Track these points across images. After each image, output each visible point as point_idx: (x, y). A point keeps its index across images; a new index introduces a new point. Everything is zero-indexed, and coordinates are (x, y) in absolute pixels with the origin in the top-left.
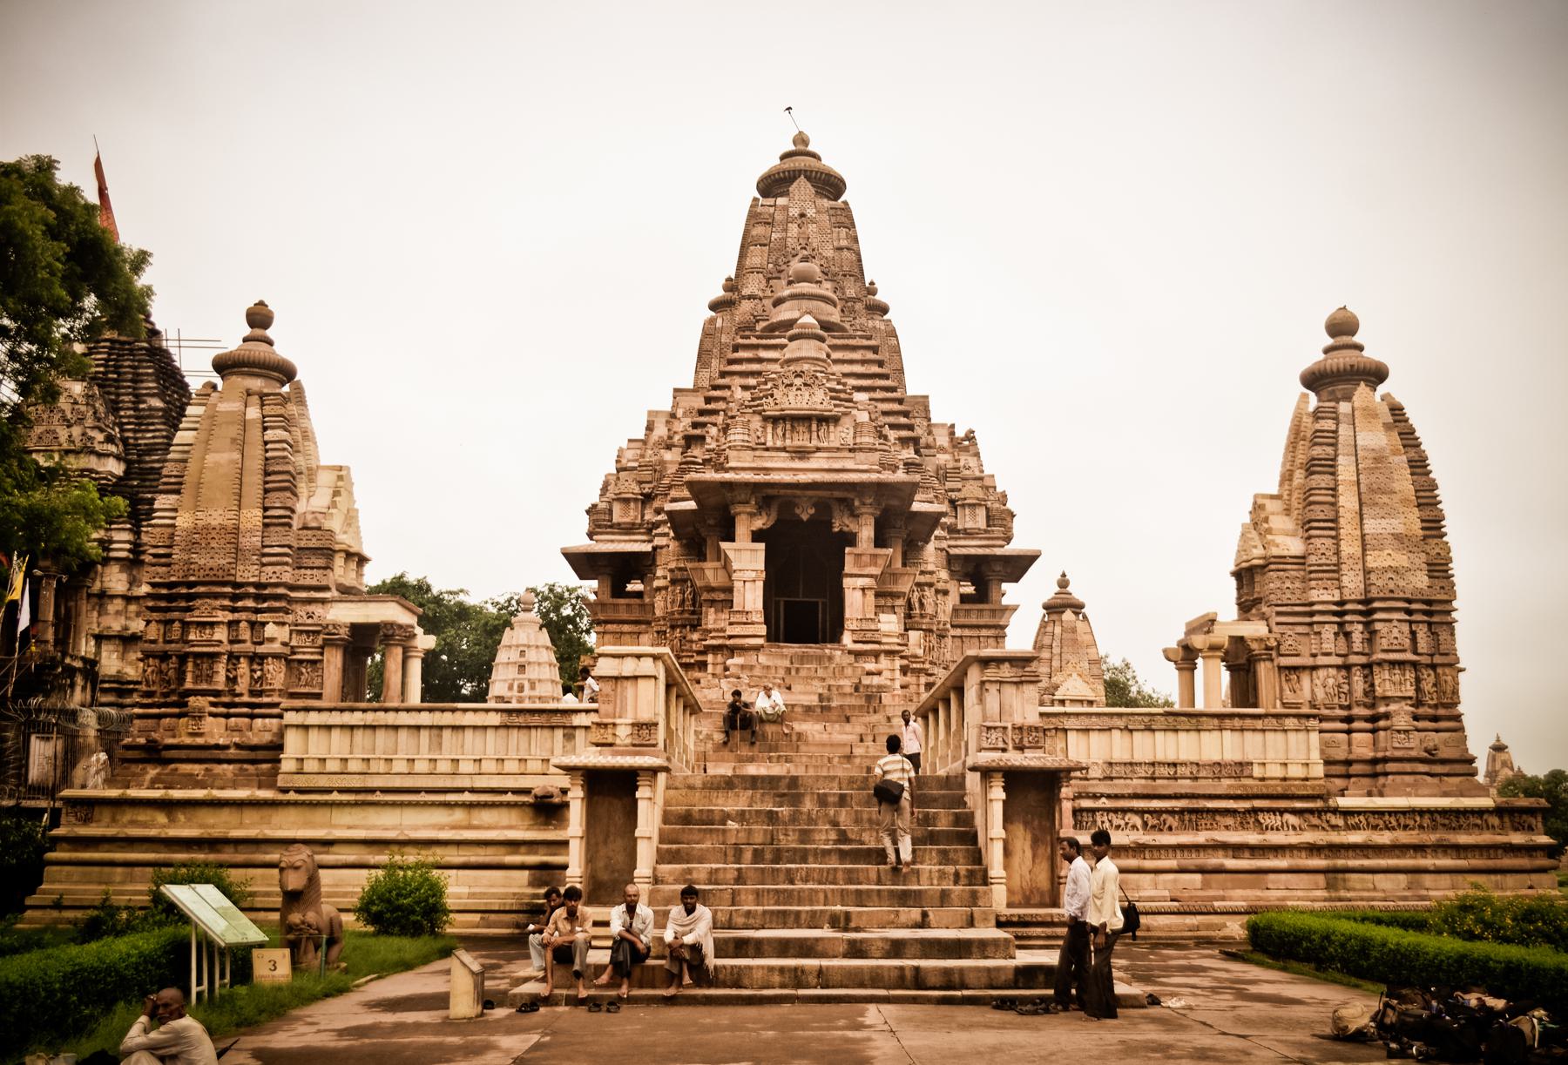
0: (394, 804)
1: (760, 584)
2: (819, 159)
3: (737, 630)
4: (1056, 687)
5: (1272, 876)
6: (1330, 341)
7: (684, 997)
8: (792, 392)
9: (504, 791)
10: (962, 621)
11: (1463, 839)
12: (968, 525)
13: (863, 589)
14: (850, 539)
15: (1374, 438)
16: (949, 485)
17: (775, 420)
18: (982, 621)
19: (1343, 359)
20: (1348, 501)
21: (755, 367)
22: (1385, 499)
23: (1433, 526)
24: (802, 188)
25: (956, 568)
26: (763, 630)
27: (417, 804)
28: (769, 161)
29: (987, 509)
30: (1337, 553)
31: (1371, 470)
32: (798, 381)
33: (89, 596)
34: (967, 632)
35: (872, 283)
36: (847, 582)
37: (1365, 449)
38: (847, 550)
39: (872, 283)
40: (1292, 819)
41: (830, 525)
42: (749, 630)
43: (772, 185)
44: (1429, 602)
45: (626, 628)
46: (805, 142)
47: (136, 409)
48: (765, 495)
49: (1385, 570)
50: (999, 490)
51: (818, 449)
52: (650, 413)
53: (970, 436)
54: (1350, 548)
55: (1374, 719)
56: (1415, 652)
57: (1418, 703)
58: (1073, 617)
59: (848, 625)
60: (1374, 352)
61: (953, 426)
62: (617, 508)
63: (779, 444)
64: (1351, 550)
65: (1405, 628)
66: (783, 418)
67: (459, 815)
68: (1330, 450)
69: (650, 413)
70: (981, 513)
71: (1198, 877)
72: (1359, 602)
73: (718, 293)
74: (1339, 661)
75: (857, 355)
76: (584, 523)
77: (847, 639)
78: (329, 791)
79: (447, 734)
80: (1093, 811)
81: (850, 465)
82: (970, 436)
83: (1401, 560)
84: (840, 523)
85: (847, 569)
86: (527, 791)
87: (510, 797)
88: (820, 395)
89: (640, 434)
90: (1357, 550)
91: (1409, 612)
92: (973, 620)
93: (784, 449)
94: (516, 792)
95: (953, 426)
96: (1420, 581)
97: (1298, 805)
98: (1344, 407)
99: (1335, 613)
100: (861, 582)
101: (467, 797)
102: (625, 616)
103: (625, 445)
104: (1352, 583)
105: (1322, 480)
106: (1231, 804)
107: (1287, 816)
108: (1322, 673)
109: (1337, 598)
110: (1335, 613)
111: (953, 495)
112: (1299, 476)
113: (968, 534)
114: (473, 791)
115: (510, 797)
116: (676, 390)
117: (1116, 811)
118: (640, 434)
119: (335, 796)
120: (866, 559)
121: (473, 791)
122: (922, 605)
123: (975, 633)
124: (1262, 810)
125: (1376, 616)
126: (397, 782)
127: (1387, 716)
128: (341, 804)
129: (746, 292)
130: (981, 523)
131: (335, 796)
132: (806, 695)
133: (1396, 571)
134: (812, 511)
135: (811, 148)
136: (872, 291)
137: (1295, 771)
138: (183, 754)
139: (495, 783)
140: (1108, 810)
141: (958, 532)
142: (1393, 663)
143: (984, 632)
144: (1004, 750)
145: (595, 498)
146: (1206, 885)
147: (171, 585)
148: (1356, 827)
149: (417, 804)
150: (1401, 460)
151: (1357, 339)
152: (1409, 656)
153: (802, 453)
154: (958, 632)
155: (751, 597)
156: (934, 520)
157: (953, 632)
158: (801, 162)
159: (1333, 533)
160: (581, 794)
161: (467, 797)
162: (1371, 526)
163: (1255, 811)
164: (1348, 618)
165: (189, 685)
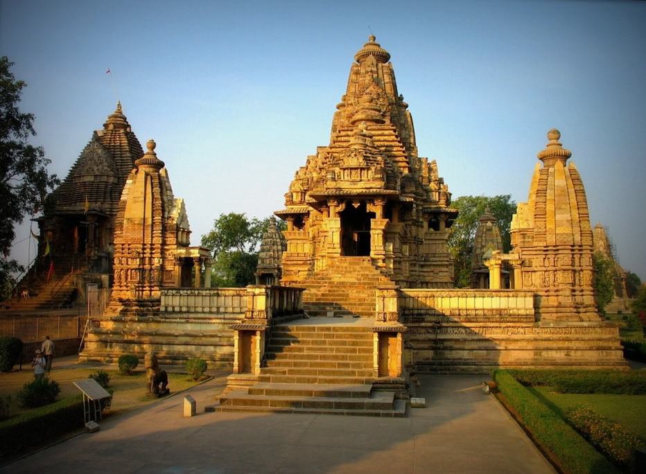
1: (339, 233)
2: (379, 46)
3: (330, 251)
4: (484, 253)
5: (512, 351)
6: (549, 142)
7: (340, 371)
8: (350, 158)
10: (428, 238)
11: (587, 337)
14: (373, 215)
15: (560, 182)
17: (344, 169)
18: (436, 238)
19: (554, 149)
20: (550, 207)
21: (346, 138)
22: (563, 206)
23: (584, 217)
24: (371, 59)
26: (339, 251)
28: (359, 48)
30: (545, 228)
31: (559, 195)
32: (353, 155)
33: (106, 229)
34: (431, 242)
35: (401, 95)
36: (372, 232)
37: (557, 186)
39: (401, 95)
40: (522, 330)
41: (366, 209)
42: (334, 251)
43: (361, 59)
44: (581, 246)
45: (299, 242)
46: (374, 39)
47: (121, 157)
48: (340, 198)
49: (563, 234)
51: (361, 181)
52: (308, 157)
53: (434, 162)
54: (550, 226)
55: (557, 291)
56: (573, 266)
57: (573, 285)
58: (491, 224)
59: (371, 248)
60: (567, 147)
61: (427, 158)
62: (294, 194)
63: (346, 178)
64: (551, 226)
65: (571, 256)
66: (347, 169)
68: (544, 187)
69: (308, 157)
71: (485, 352)
72: (554, 246)
73: (341, 102)
74: (545, 269)
75: (386, 132)
76: (284, 200)
77: (372, 254)
78: (176, 318)
79: (215, 298)
80: (447, 327)
81: (373, 185)
82: (434, 162)
83: (568, 231)
84: (370, 208)
85: (372, 227)
88: (361, 160)
89: (326, 141)
90: (552, 226)
91: (572, 250)
93: (348, 181)
95: (427, 158)
96: (577, 238)
97: (524, 325)
98: (551, 170)
99: (544, 251)
102: (298, 237)
103: (298, 169)
104: (551, 239)
105: (542, 199)
106: (497, 324)
107: (519, 329)
108: (539, 273)
109: (545, 245)
110: (544, 251)
112: (534, 196)
116: (318, 147)
117: (455, 327)
118: (304, 165)
119: (178, 320)
120: (379, 223)
121: (224, 319)
122: (410, 232)
123: (434, 242)
124: (510, 327)
125: (560, 252)
126: (199, 315)
127: (562, 290)
128: (180, 323)
129: (350, 102)
132: (350, 279)
133: (567, 234)
135: (376, 42)
136: (401, 98)
137: (522, 312)
139: (232, 316)
140: (453, 327)
142: (564, 270)
143: (437, 242)
144: (385, 321)
145: (287, 191)
146: (488, 354)
147: (123, 245)
148: (545, 333)
150: (572, 190)
151: (560, 141)
152: (570, 267)
153: (354, 182)
154: (427, 242)
155: (337, 238)
156: (412, 203)
158: (372, 48)
159: (544, 220)
160: (238, 337)
162: (558, 217)
163: (507, 327)
164: (548, 253)
165: (129, 280)
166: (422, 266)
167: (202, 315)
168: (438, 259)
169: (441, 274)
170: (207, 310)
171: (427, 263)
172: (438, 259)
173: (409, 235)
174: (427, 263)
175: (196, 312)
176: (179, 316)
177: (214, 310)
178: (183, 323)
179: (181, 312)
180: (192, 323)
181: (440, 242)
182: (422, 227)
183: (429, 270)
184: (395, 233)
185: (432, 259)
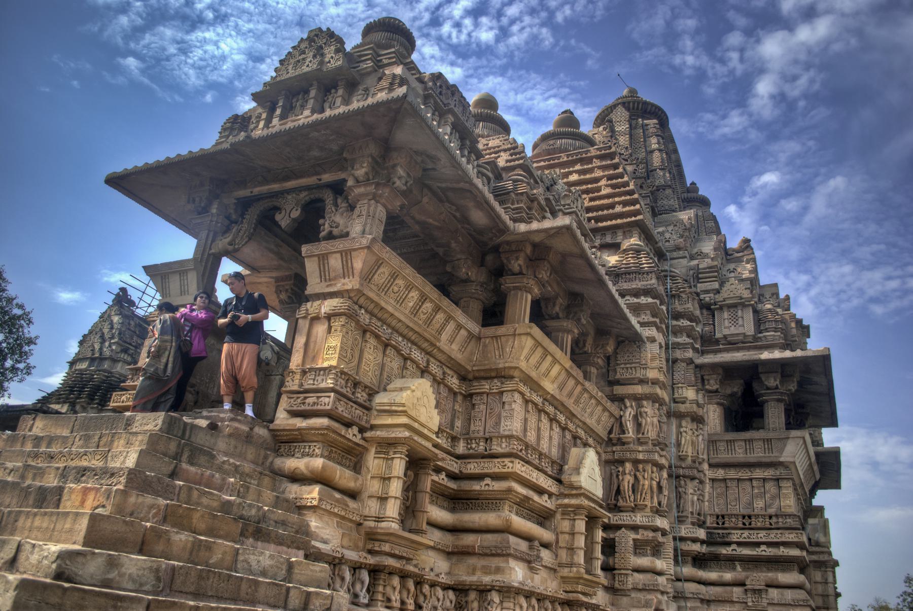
12: (726, 332)
13: (329, 317)
16: (701, 287)
18: (753, 457)
25: (713, 385)
29: (756, 312)
34: (732, 474)
38: (305, 249)
50: (782, 295)
70: (749, 316)
92: (739, 454)
100: (327, 306)
111: (707, 298)
113: (732, 344)
122: (639, 426)
123: (744, 474)
130: (748, 328)
134: (296, 214)
141: (717, 342)
143: (759, 473)
154: (720, 473)
157: (709, 473)
166: (699, 561)
168: (762, 536)
169: (774, 593)
171: (724, 551)
172: (762, 534)
173: (631, 434)
174: (724, 551)
181: (769, 473)
182: (698, 420)
183: (728, 576)
184: (503, 375)
185: (735, 536)
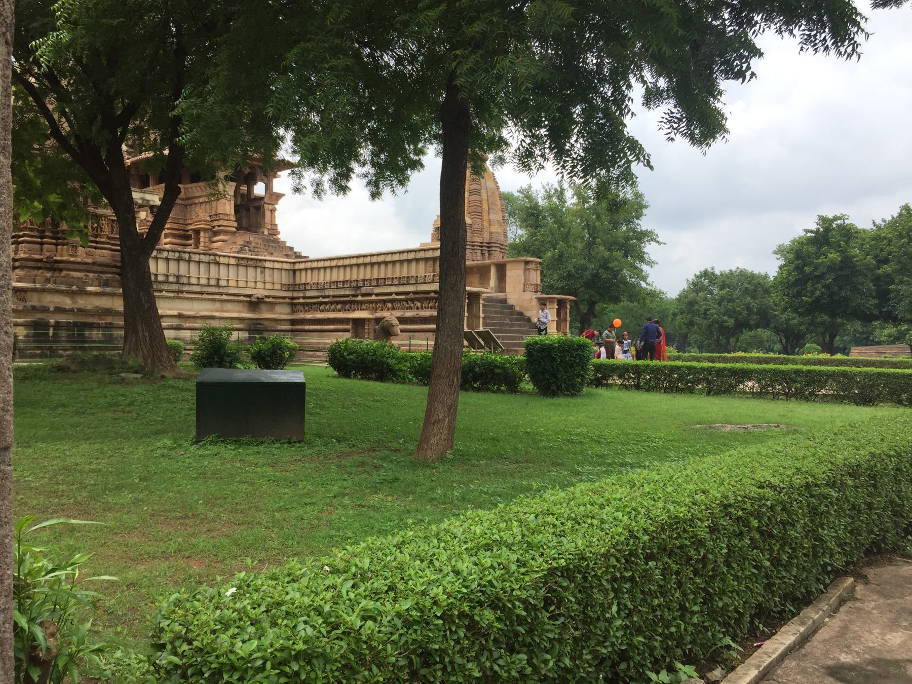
0: (191, 299)
9: (239, 295)
27: (202, 299)
67: (218, 305)
86: (250, 296)
87: (242, 298)
94: (244, 296)
101: (224, 297)
114: (227, 294)
115: (242, 298)
121: (227, 294)
128: (166, 297)
131: (164, 294)
138: (72, 266)
139: (236, 291)
149: (202, 299)
161: (224, 297)
167: (198, 289)
170: (203, 281)
175: (189, 284)
176: (166, 287)
177: (213, 282)
178: (170, 298)
179: (167, 282)
180: (184, 298)
